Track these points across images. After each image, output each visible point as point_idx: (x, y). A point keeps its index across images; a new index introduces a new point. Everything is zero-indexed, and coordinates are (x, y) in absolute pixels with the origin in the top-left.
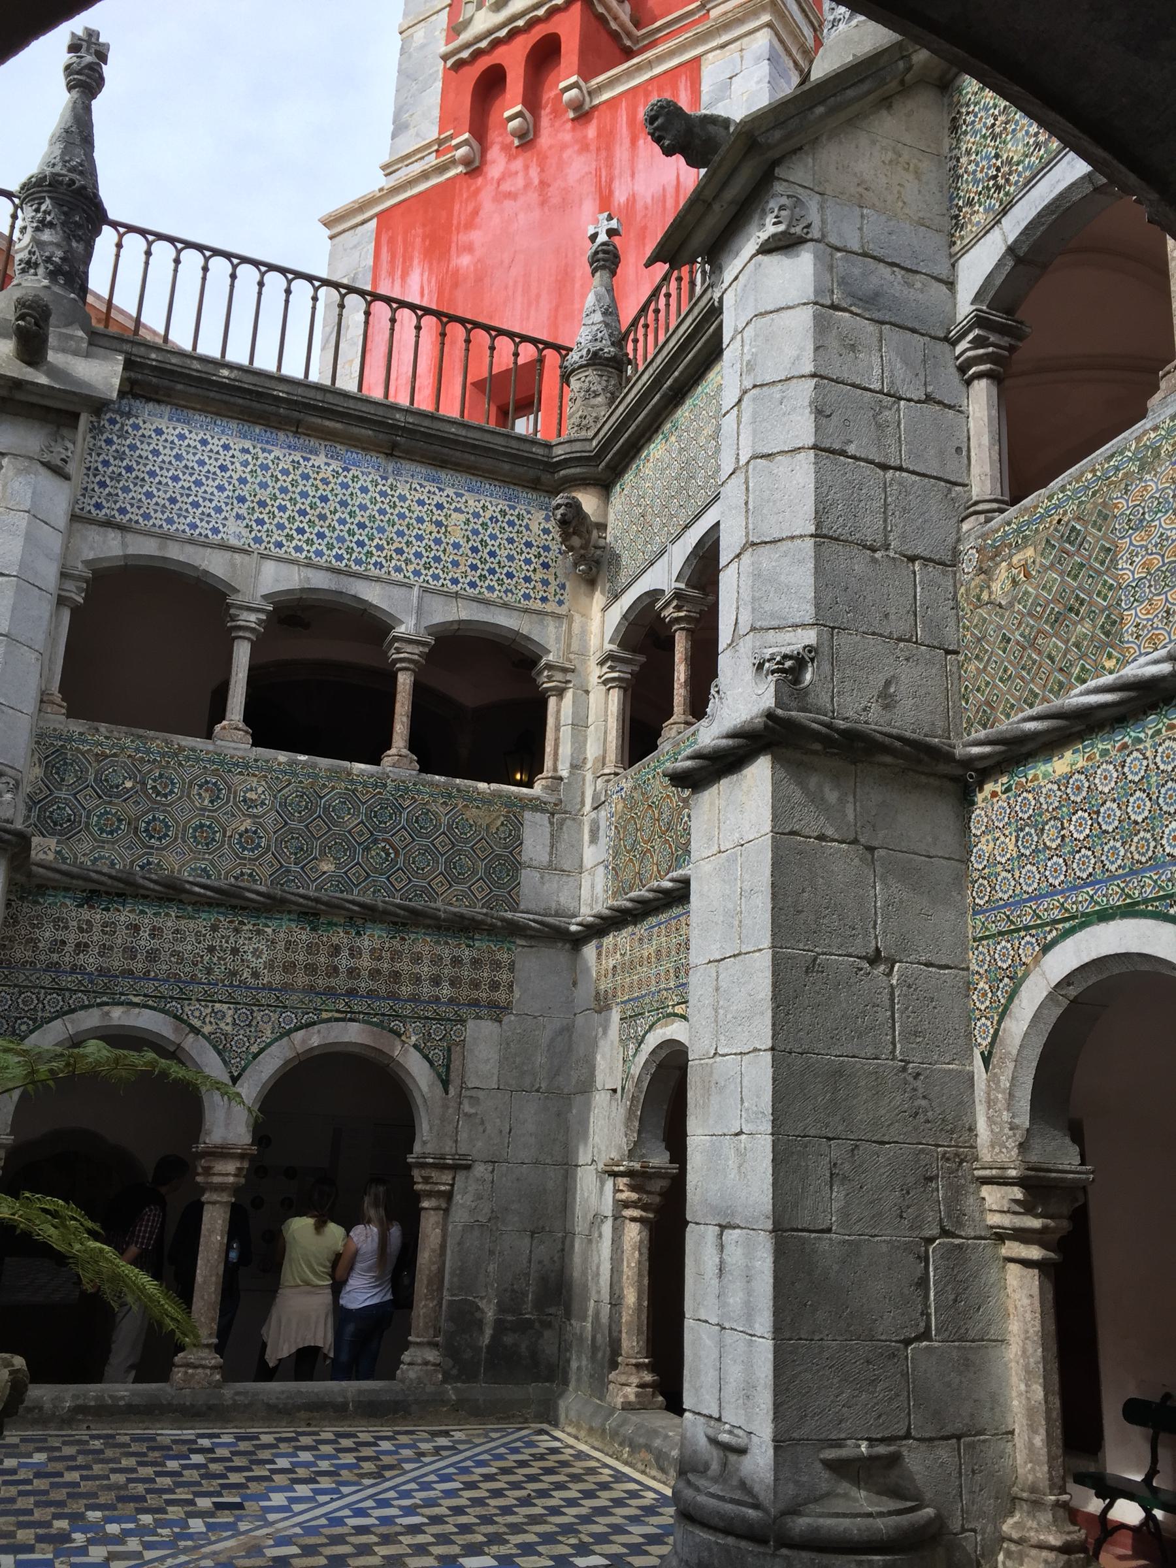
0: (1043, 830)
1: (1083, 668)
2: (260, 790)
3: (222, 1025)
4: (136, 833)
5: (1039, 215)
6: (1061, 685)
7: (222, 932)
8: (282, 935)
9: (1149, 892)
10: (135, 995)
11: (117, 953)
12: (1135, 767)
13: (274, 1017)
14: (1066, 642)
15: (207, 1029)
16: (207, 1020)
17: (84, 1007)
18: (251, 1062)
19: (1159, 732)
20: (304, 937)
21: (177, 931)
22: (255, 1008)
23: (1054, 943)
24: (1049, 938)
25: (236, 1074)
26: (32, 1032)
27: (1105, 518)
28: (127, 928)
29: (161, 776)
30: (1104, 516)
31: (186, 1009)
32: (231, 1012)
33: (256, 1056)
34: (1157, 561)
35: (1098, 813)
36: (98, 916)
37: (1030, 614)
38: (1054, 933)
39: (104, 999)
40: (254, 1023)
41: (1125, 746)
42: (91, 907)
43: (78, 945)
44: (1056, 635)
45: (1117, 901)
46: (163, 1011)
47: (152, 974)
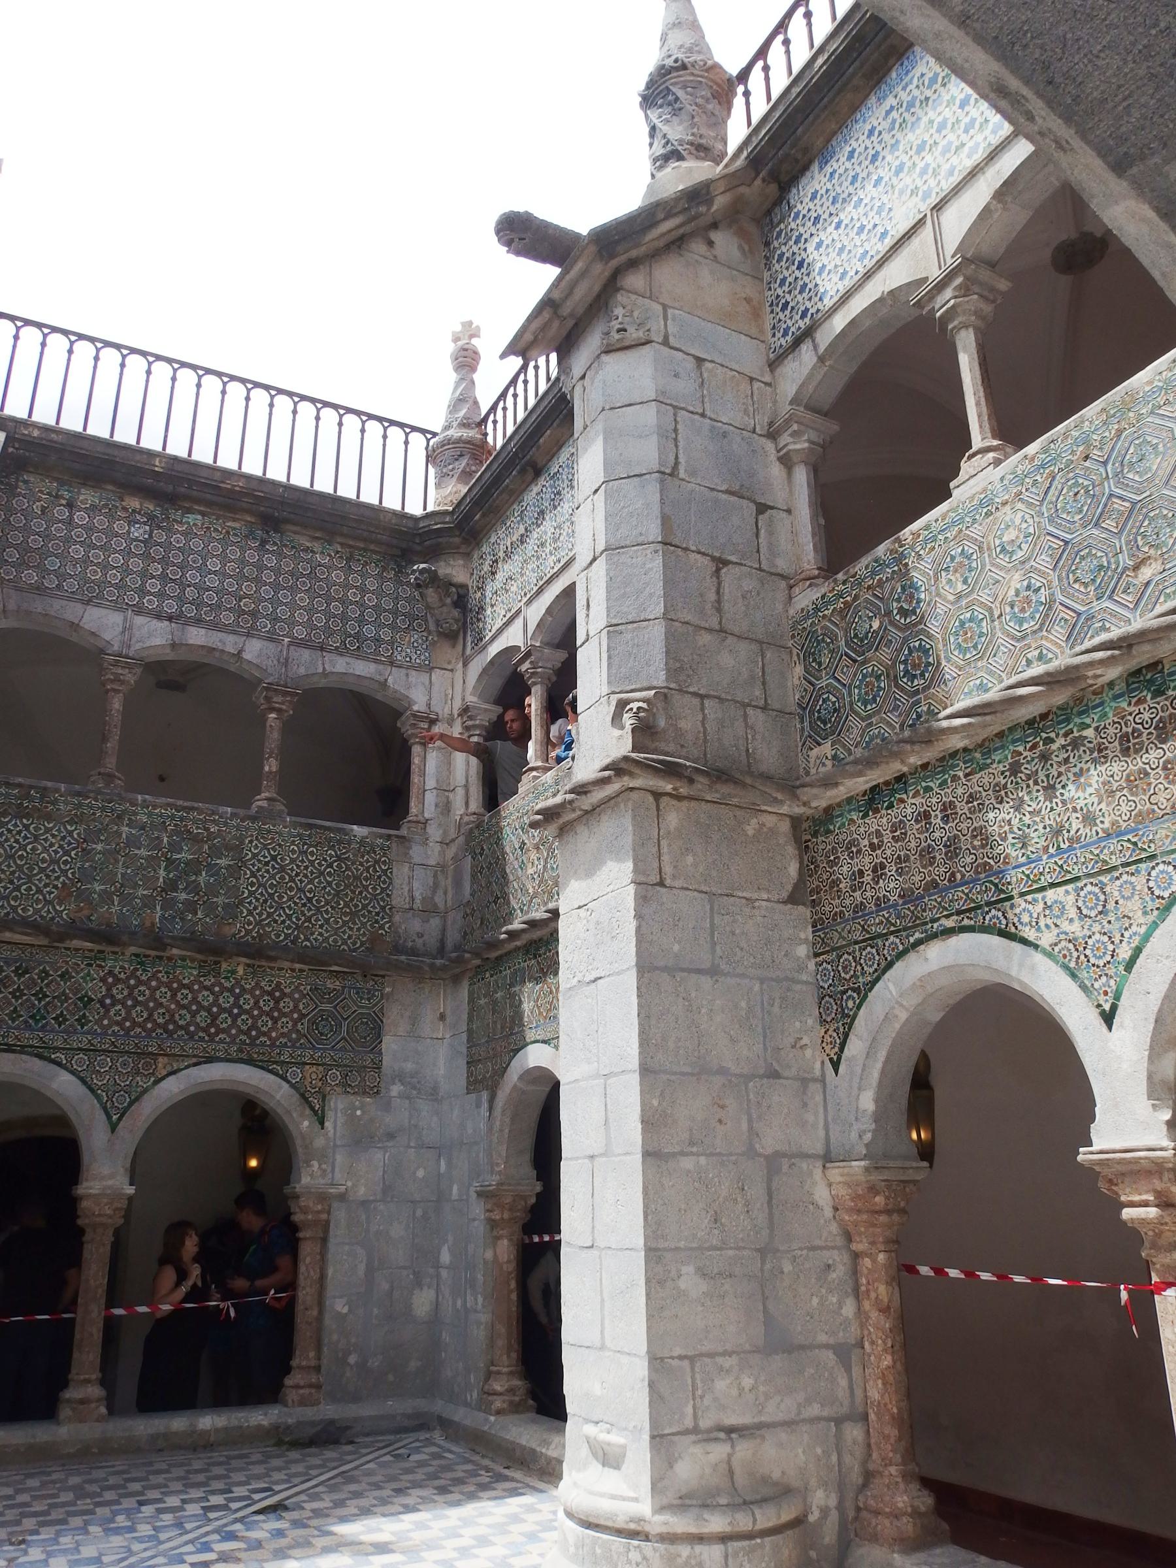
2: (1018, 521)
3: (1065, 926)
4: (897, 686)
7: (1027, 769)
8: (1111, 730)
10: (947, 917)
11: (915, 863)
13: (1139, 881)
15: (1046, 939)
16: (1042, 924)
17: (901, 955)
18: (1125, 980)
20: (1146, 716)
21: (972, 798)
22: (1105, 879)
25: (1107, 1007)
26: (859, 1007)
28: (917, 821)
29: (903, 588)
31: (1010, 915)
32: (1071, 898)
33: (1130, 965)
36: (884, 820)
39: (917, 935)
40: (1111, 905)
42: (877, 811)
43: (875, 870)
46: (984, 929)
47: (959, 876)
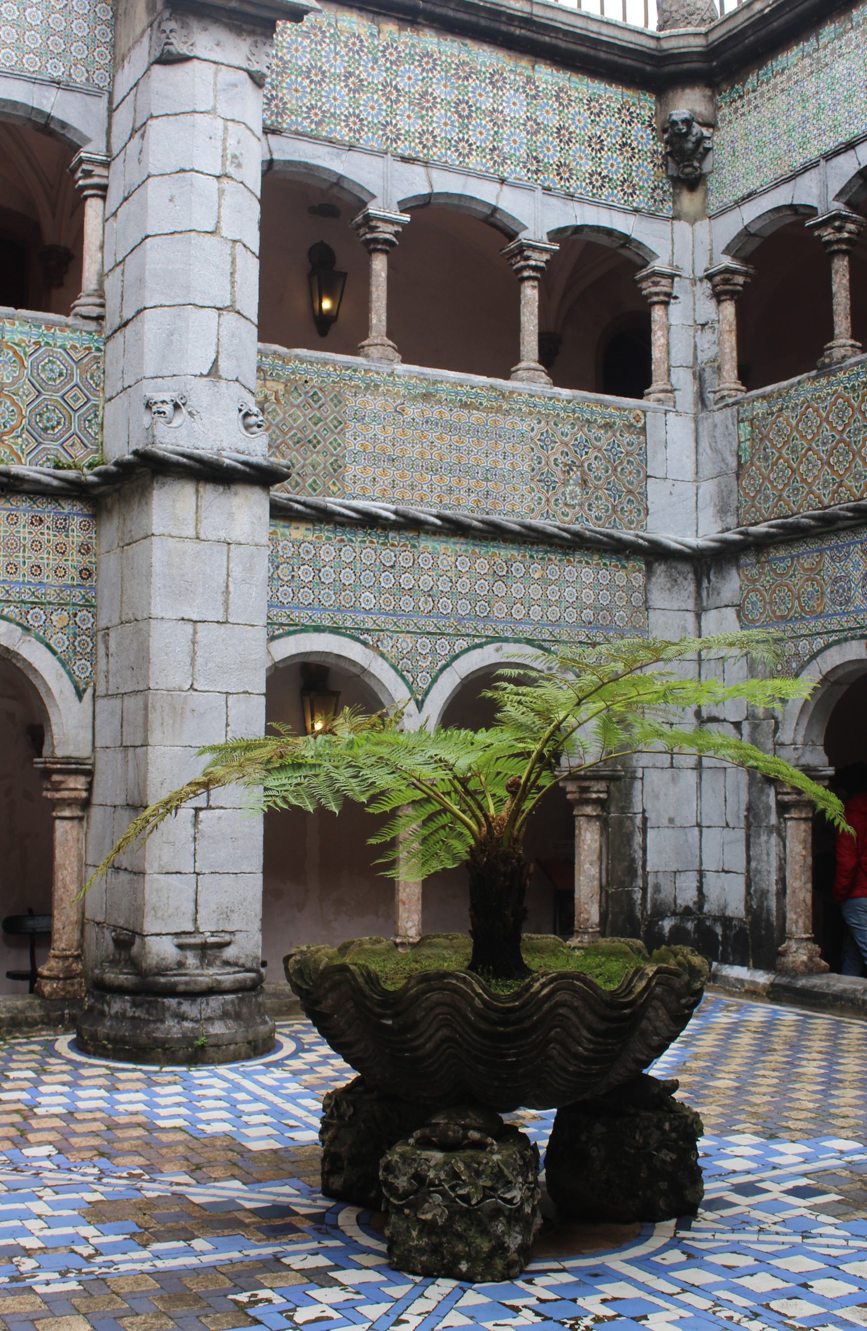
0: (278, 567)
1: (315, 482)
5: (300, 163)
6: (297, 484)
9: (348, 624)
12: (347, 554)
14: (305, 460)
19: (364, 542)
23: (279, 637)
24: (277, 633)
27: (340, 402)
30: (338, 400)
34: (370, 449)
35: (320, 571)
37: (277, 426)
38: (281, 631)
41: (342, 540)
44: (297, 451)
45: (327, 623)
